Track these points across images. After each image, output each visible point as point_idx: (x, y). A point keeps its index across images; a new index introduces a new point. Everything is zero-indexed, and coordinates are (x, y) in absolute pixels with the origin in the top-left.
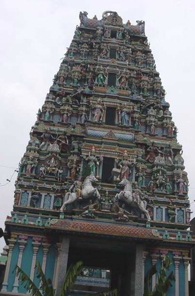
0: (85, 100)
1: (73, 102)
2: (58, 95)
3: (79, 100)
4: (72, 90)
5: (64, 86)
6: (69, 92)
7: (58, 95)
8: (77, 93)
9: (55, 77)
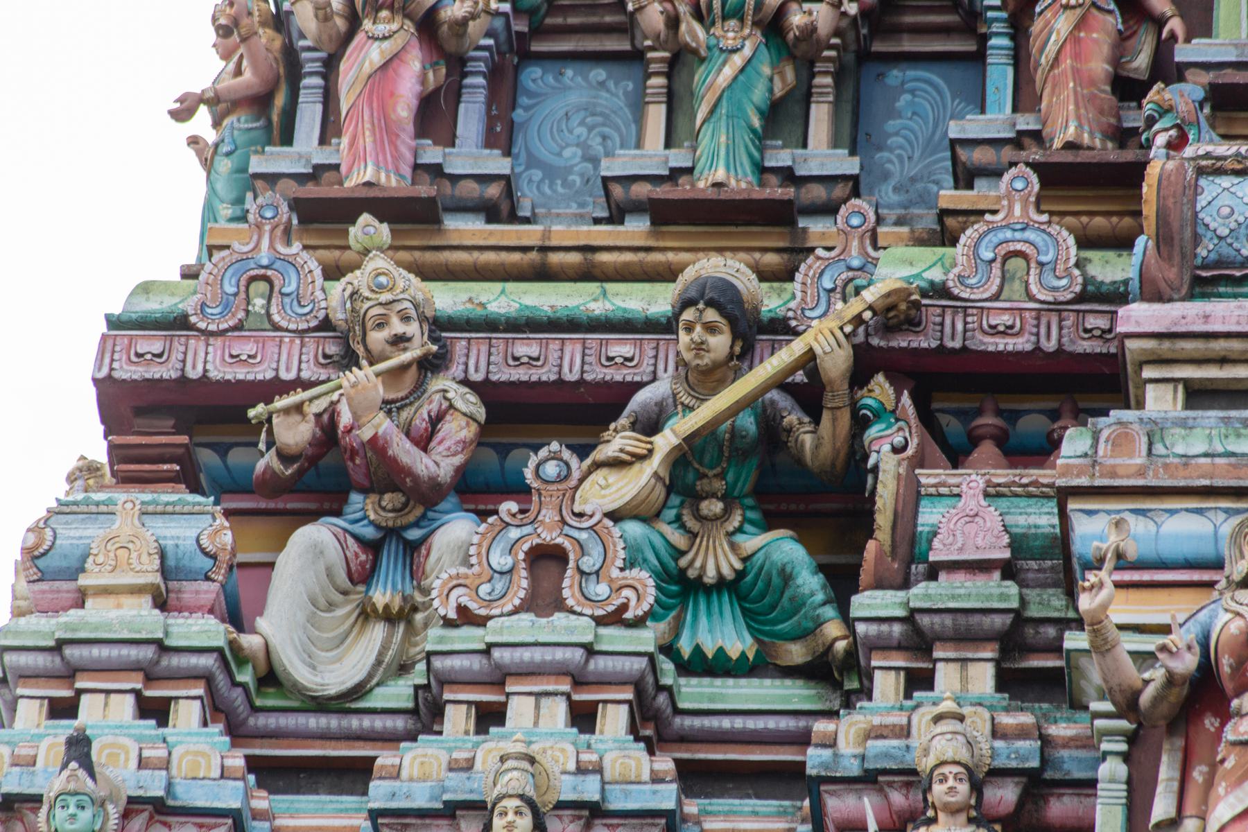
0: (968, 513)
1: (681, 588)
2: (326, 476)
3: (831, 508)
4: (654, 300)
5: (465, 228)
6: (569, 361)
7: (326, 476)
8: (776, 361)
9: (228, 30)
